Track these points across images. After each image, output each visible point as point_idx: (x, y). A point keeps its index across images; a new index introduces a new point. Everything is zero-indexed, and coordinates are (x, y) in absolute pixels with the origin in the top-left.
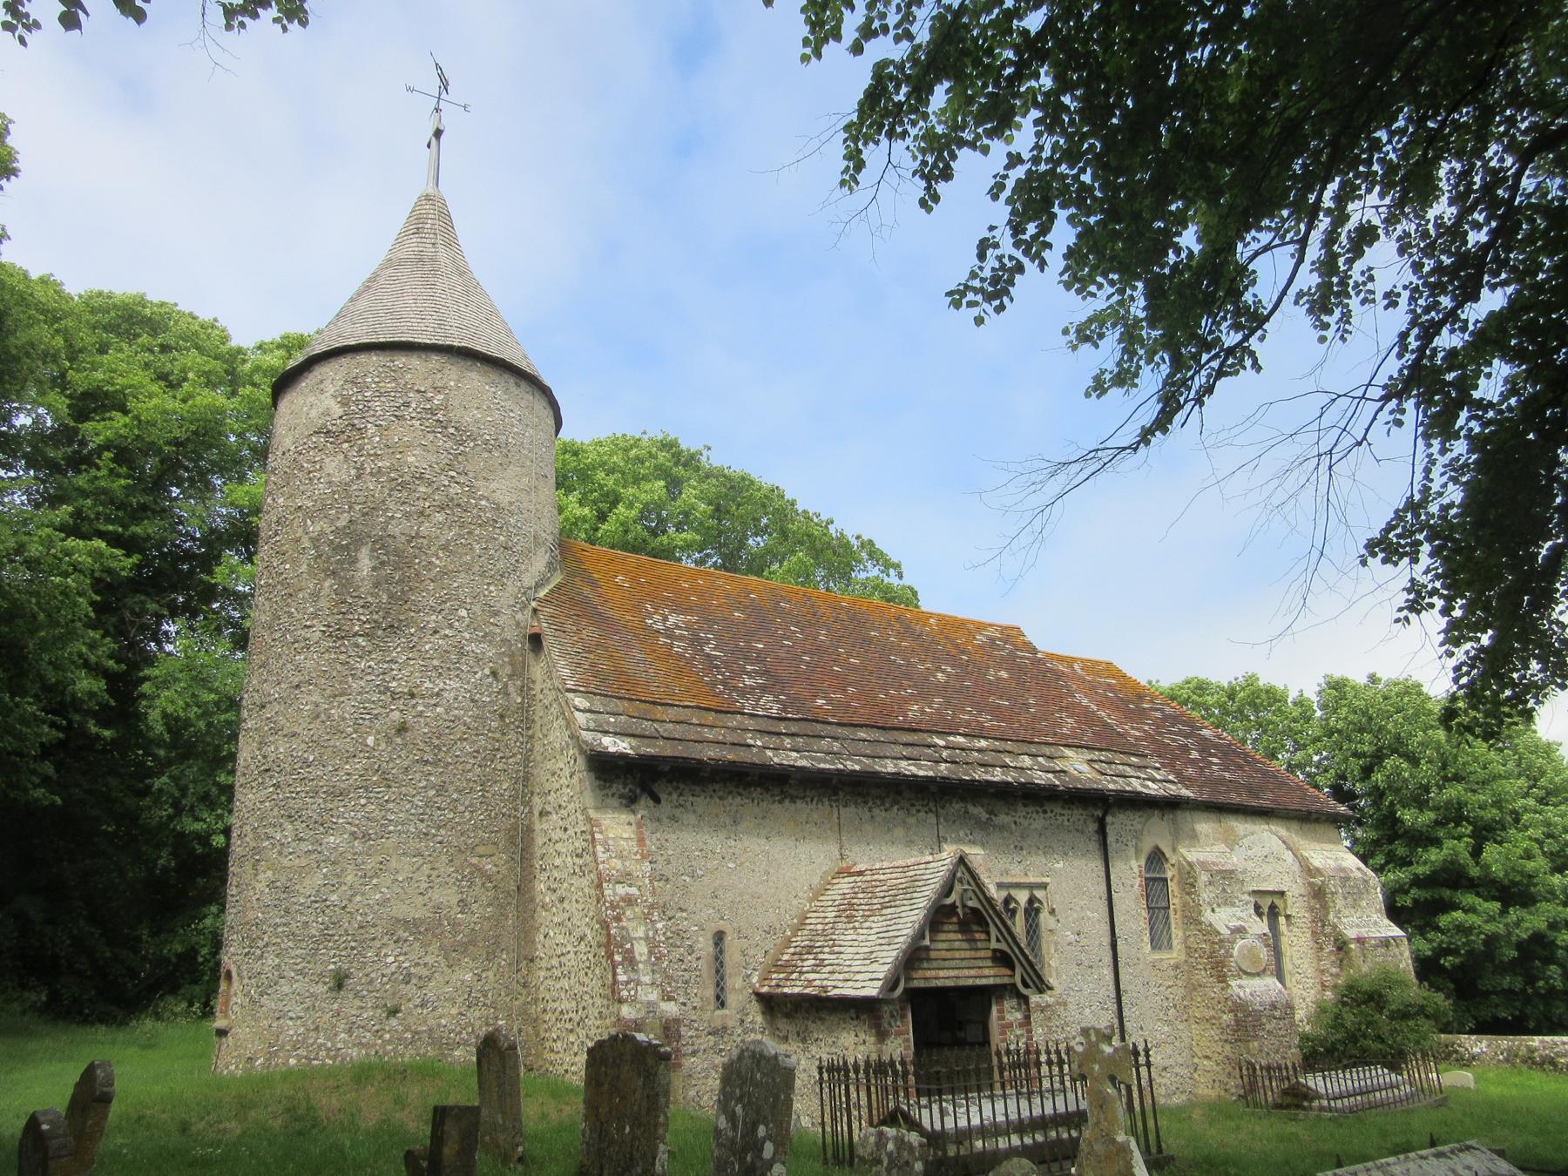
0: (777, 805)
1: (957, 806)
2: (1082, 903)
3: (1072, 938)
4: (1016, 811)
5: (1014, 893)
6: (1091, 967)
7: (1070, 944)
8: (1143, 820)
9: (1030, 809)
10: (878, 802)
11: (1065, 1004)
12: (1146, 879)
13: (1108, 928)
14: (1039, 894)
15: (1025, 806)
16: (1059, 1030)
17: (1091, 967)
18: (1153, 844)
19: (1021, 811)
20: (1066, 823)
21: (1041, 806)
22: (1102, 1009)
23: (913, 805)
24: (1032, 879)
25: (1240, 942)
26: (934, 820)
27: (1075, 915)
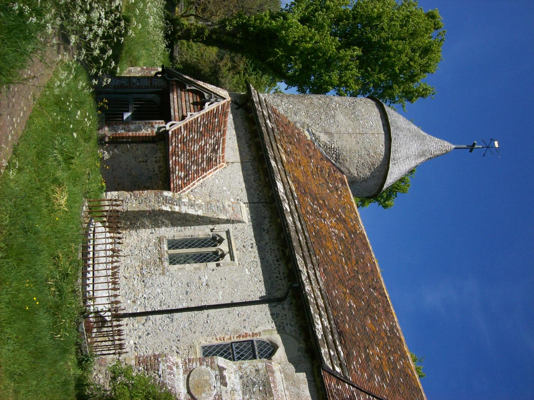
0: (245, 142)
1: (266, 213)
2: (227, 287)
3: (204, 280)
4: (273, 244)
5: (226, 242)
6: (187, 294)
7: (200, 279)
8: (293, 334)
9: (276, 251)
10: (258, 178)
11: (163, 274)
12: (252, 341)
13: (214, 303)
14: (227, 257)
15: (278, 249)
16: (148, 270)
17: (187, 294)
18: (279, 346)
19: (275, 247)
20: (275, 275)
21: (280, 259)
22: (161, 302)
23: (260, 192)
24: (235, 253)
25: (213, 373)
26: (255, 201)
27: (218, 282)
